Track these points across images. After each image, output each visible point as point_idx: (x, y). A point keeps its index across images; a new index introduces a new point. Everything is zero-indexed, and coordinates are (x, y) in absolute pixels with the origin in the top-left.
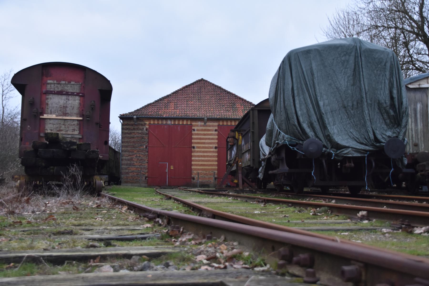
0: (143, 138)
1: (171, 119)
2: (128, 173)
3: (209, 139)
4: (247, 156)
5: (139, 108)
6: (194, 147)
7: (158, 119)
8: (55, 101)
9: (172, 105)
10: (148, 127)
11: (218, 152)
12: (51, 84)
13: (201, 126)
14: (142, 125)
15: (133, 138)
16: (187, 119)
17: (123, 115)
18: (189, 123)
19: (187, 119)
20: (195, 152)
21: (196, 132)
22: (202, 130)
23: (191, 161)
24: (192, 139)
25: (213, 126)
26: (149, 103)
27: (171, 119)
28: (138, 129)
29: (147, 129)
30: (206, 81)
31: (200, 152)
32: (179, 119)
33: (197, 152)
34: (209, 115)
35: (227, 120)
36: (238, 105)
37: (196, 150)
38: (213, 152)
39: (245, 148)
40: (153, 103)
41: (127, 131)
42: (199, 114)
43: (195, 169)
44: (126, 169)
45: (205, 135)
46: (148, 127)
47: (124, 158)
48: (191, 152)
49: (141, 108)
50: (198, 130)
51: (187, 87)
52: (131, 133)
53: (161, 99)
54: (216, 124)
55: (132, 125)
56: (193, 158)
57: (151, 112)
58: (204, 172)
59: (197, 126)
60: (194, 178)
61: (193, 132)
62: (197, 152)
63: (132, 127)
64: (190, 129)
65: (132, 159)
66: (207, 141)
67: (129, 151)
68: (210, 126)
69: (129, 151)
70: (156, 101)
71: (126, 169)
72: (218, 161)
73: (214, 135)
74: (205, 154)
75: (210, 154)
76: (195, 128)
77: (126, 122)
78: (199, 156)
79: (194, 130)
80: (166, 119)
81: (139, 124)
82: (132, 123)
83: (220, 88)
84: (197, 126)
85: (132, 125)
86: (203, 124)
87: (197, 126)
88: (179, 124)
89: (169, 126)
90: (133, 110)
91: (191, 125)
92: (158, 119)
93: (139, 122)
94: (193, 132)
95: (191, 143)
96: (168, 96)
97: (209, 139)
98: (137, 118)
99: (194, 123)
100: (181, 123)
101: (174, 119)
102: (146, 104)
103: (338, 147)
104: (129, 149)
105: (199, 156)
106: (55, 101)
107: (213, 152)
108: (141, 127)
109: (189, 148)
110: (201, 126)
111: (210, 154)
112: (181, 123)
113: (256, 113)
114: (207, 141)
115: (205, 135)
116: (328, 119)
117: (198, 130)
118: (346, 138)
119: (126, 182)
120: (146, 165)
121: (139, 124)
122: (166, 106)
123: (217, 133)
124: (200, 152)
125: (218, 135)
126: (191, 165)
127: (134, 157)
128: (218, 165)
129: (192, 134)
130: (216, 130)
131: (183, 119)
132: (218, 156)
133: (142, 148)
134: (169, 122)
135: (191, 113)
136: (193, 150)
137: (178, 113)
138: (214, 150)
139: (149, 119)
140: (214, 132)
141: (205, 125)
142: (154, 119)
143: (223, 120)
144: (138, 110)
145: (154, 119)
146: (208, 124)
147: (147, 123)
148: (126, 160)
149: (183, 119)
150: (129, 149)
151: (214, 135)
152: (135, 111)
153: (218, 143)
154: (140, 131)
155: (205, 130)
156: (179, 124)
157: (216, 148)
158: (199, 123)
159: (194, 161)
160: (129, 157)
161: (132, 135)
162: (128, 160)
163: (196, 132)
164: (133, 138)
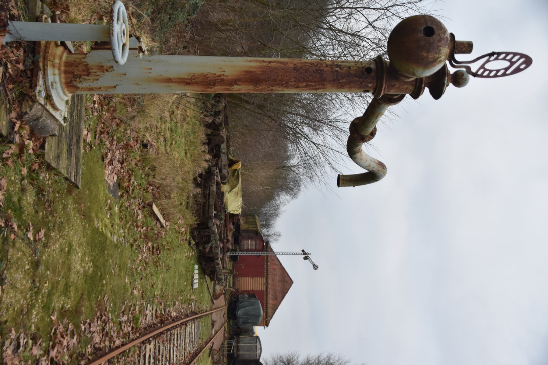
1: (267, 267)
9: (276, 267)
12: (258, 242)
19: (267, 275)
30: (291, 285)
34: (269, 286)
35: (267, 295)
36: (276, 301)
42: (270, 281)
51: (287, 274)
59: (263, 280)
64: (262, 276)
74: (250, 284)
80: (267, 264)
83: (287, 292)
89: (264, 266)
91: (264, 277)
92: (267, 260)
96: (281, 264)
103: (238, 310)
106: (254, 243)
109: (253, 276)
118: (240, 313)
122: (274, 264)
131: (267, 273)
134: (265, 266)
135: (269, 276)
137: (270, 270)
158: (265, 281)
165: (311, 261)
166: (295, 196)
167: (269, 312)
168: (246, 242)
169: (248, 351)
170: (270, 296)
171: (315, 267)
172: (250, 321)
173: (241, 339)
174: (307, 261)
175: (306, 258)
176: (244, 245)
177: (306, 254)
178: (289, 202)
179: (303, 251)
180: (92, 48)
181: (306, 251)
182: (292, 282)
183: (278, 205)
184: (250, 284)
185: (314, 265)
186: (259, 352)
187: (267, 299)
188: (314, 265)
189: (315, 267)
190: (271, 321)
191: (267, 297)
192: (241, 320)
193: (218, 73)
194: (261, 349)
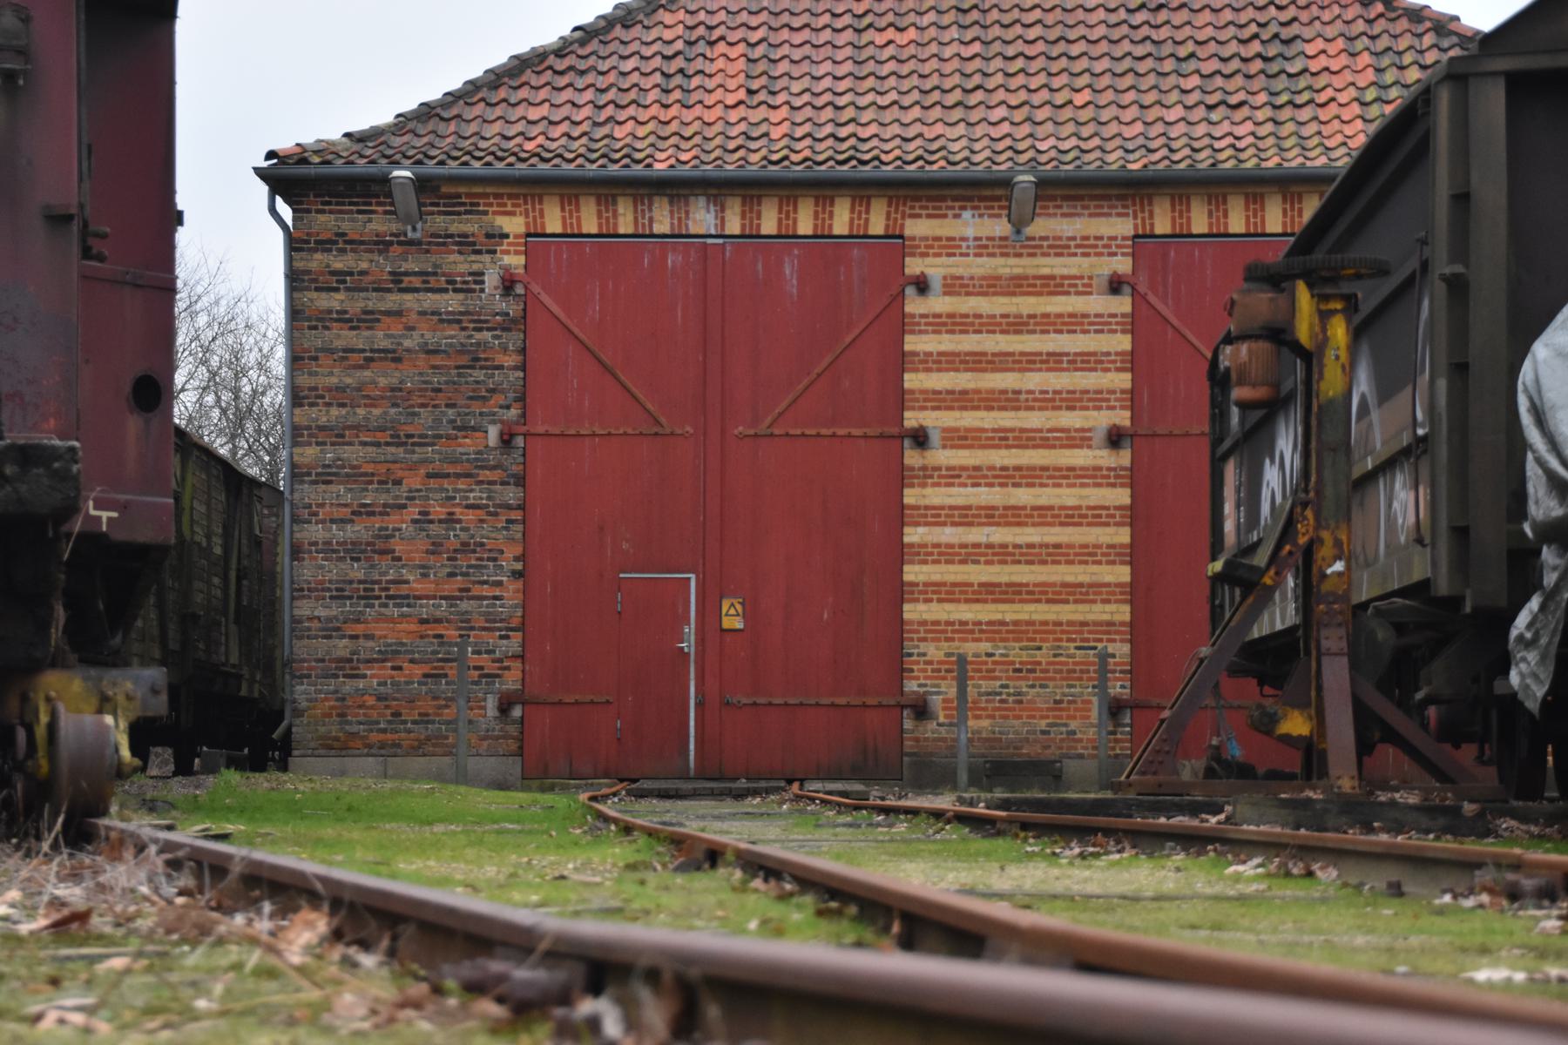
0: (475, 358)
1: (716, 188)
2: (348, 667)
3: (1053, 361)
4: (1403, 503)
5: (434, 94)
6: (920, 439)
7: (607, 189)
10: (516, 261)
11: (1134, 478)
13: (983, 247)
14: (465, 244)
15: (394, 356)
16: (862, 189)
17: (300, 156)
18: (877, 226)
19: (862, 189)
20: (928, 475)
21: (938, 303)
22: (991, 286)
23: (899, 554)
24: (902, 361)
25: (1088, 246)
26: (523, 48)
27: (716, 188)
28: (429, 282)
29: (508, 284)
31: (977, 476)
32: (788, 189)
33: (953, 476)
34: (1056, 146)
35: (1216, 185)
37: (941, 456)
38: (1092, 476)
39: (1378, 432)
40: (562, 49)
41: (334, 301)
42: (962, 144)
43: (937, 630)
44: (331, 630)
45: (1017, 325)
46: (516, 261)
47: (315, 532)
48: (901, 477)
49: (452, 98)
50: (953, 286)
52: (369, 319)
54: (1121, 226)
55: (381, 245)
56: (913, 535)
57: (544, 129)
58: (1017, 653)
59: (952, 251)
60: (921, 710)
61: (915, 305)
62: (953, 476)
63: (382, 266)
64: (888, 274)
65: (380, 547)
66: (1034, 381)
67: (357, 477)
68: (1060, 247)
69: (357, 477)
70: (586, 33)
71: (331, 630)
72: (1134, 555)
73: (1100, 324)
75: (1067, 496)
76: (934, 268)
77: (325, 222)
78: (964, 516)
79: (922, 285)
80: (677, 188)
81: (443, 240)
82: (379, 224)
84: (952, 251)
85: (381, 245)
86: (1000, 227)
87: (950, 246)
88: (787, 235)
89: (703, 249)
90: (383, 116)
92: (607, 189)
93: (440, 222)
94: (915, 305)
95: (901, 399)
97: (1053, 361)
98: (423, 185)
99: (917, 228)
100: (805, 226)
101: (750, 189)
102: (498, 57)
104: (353, 453)
105: (964, 516)
107: (1092, 476)
108: (458, 263)
110: (983, 247)
111: (1067, 496)
112: (805, 226)
113: (1492, 103)
114: (1034, 381)
115: (1017, 325)
117: (953, 286)
119: (338, 746)
120: (512, 593)
121: (443, 240)
122: (678, 77)
123: (1122, 304)
124: (977, 476)
125: (1133, 324)
126: (900, 592)
127: (403, 522)
128: (1136, 593)
129: (903, 325)
130: (1115, 285)
131: (823, 188)
132: (1135, 515)
133: (467, 446)
134: (702, 218)
135: (895, 136)
136: (912, 458)
138: (1103, 457)
139: (531, 188)
140: (1099, 303)
142: (570, 188)
143: (1178, 186)
144: (427, 112)
145: (570, 188)
146: (1040, 227)
147: (514, 225)
148: (328, 549)
149: (823, 188)
150: (353, 453)
151: (1100, 324)
152: (405, 123)
153: (1133, 398)
154: (452, 302)
155: (1018, 285)
156: (787, 235)
157: (1115, 439)
158: (970, 224)
159: (926, 553)
160: (358, 530)
161: (380, 338)
162: (355, 551)
163: (938, 303)
164: (394, 356)
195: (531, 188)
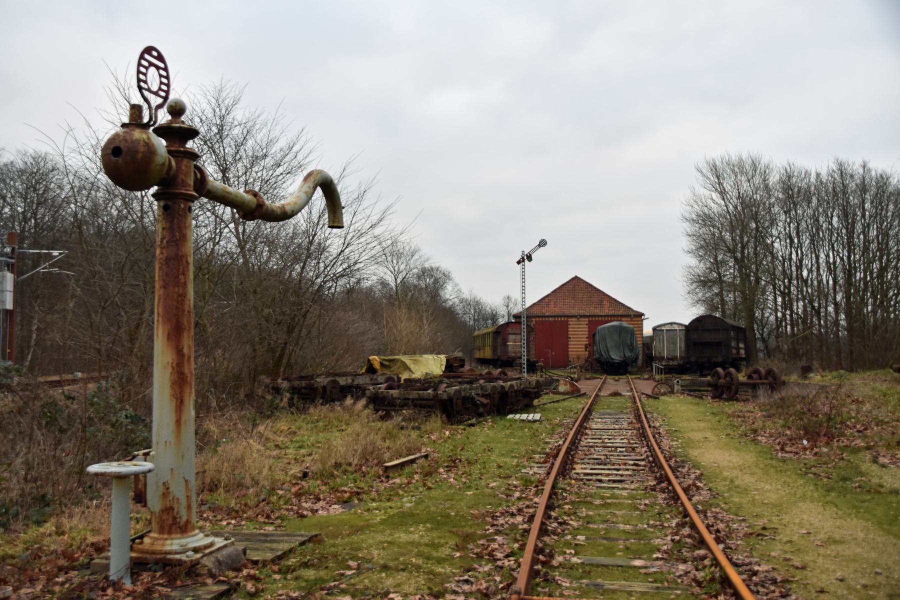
1: (551, 317)
8: (511, 337)
9: (552, 303)
12: (510, 330)
16: (564, 316)
19: (564, 316)
27: (551, 317)
32: (558, 316)
34: (581, 312)
35: (595, 316)
36: (605, 302)
42: (573, 312)
51: (563, 285)
53: (543, 299)
57: (536, 311)
59: (572, 321)
64: (566, 324)
74: (578, 341)
80: (548, 317)
84: (572, 321)
89: (550, 322)
92: (542, 317)
96: (548, 295)
101: (555, 316)
106: (511, 337)
109: (568, 338)
116: (610, 350)
118: (616, 356)
122: (548, 305)
131: (561, 316)
135: (567, 313)
141: (578, 320)
142: (539, 317)
143: (592, 316)
149: (561, 316)
158: (574, 319)
165: (534, 250)
166: (447, 276)
167: (621, 312)
168: (510, 349)
169: (675, 343)
170: (597, 312)
171: (543, 243)
172: (629, 342)
173: (658, 355)
174: (533, 256)
175: (529, 258)
176: (515, 352)
177: (523, 258)
178: (457, 285)
179: (519, 263)
180: (145, 506)
181: (519, 258)
182: (576, 278)
183: (461, 301)
184: (578, 341)
185: (539, 246)
186: (676, 327)
187: (602, 316)
188: (539, 246)
189: (543, 243)
190: (635, 309)
191: (599, 316)
192: (628, 354)
193: (170, 370)
194: (671, 324)
195: (535, 317)
